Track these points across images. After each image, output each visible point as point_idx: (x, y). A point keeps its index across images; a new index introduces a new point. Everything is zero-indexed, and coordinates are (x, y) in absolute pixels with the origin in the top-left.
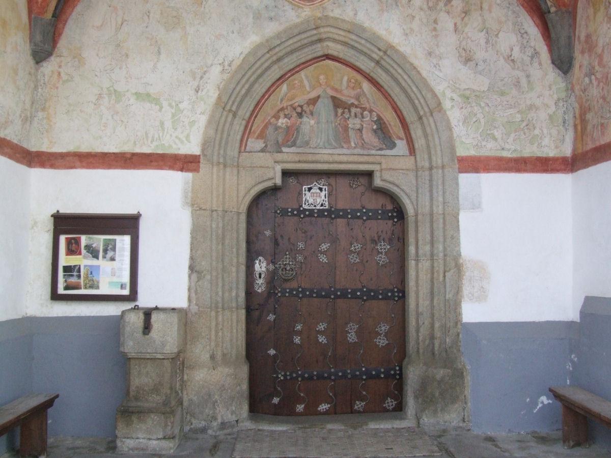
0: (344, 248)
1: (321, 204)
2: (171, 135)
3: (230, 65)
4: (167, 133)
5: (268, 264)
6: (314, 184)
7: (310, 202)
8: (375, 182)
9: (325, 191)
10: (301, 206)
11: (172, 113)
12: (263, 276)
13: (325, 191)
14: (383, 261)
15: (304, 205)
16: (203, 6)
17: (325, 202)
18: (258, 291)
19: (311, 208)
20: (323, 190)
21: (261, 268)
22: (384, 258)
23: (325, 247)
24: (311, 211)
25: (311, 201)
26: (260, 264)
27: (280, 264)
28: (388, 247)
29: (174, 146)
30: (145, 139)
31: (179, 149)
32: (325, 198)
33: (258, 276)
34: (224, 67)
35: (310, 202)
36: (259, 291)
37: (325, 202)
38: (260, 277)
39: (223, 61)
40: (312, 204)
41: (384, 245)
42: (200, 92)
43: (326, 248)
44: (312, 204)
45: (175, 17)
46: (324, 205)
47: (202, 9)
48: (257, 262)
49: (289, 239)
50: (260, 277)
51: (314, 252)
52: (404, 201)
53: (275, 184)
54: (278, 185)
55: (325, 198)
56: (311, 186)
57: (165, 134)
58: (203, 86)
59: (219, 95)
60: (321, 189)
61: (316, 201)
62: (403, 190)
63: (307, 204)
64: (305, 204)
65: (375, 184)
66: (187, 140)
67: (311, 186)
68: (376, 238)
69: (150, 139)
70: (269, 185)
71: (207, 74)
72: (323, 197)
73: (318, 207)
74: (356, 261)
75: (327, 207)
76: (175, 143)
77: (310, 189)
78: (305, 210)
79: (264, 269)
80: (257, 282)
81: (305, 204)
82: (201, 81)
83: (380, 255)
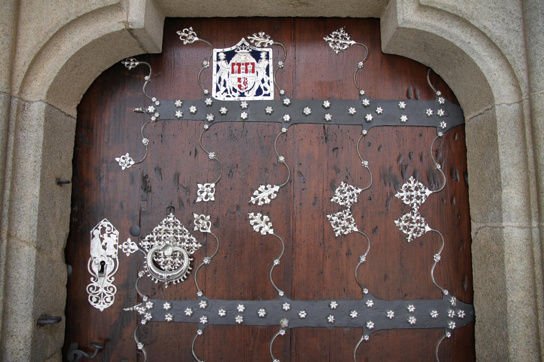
0: (315, 198)
1: (256, 87)
5: (122, 239)
6: (239, 44)
7: (229, 86)
8: (400, 17)
9: (267, 58)
10: (209, 95)
12: (109, 269)
13: (267, 58)
14: (415, 231)
15: (214, 94)
17: (266, 84)
18: (97, 306)
19: (232, 99)
20: (263, 55)
21: (104, 248)
22: (418, 221)
23: (265, 194)
24: (235, 106)
25: (232, 82)
26: (102, 239)
27: (150, 240)
28: (428, 192)
32: (268, 74)
33: (96, 269)
35: (229, 86)
36: (101, 307)
37: (266, 84)
38: (102, 271)
40: (235, 91)
41: (416, 189)
43: (269, 196)
44: (235, 91)
46: (264, 92)
48: (96, 232)
49: (177, 176)
50: (102, 271)
51: (238, 207)
52: (480, 65)
53: (127, 23)
54: (135, 27)
55: (268, 74)
56: (234, 48)
60: (256, 55)
61: (245, 83)
62: (482, 34)
63: (222, 89)
64: (218, 90)
65: (400, 22)
67: (234, 48)
68: (396, 171)
70: (114, 30)
72: (262, 74)
73: (251, 96)
74: (349, 230)
75: (271, 98)
77: (229, 56)
78: (217, 104)
79: (112, 251)
80: (95, 284)
81: (218, 90)
83: (409, 215)
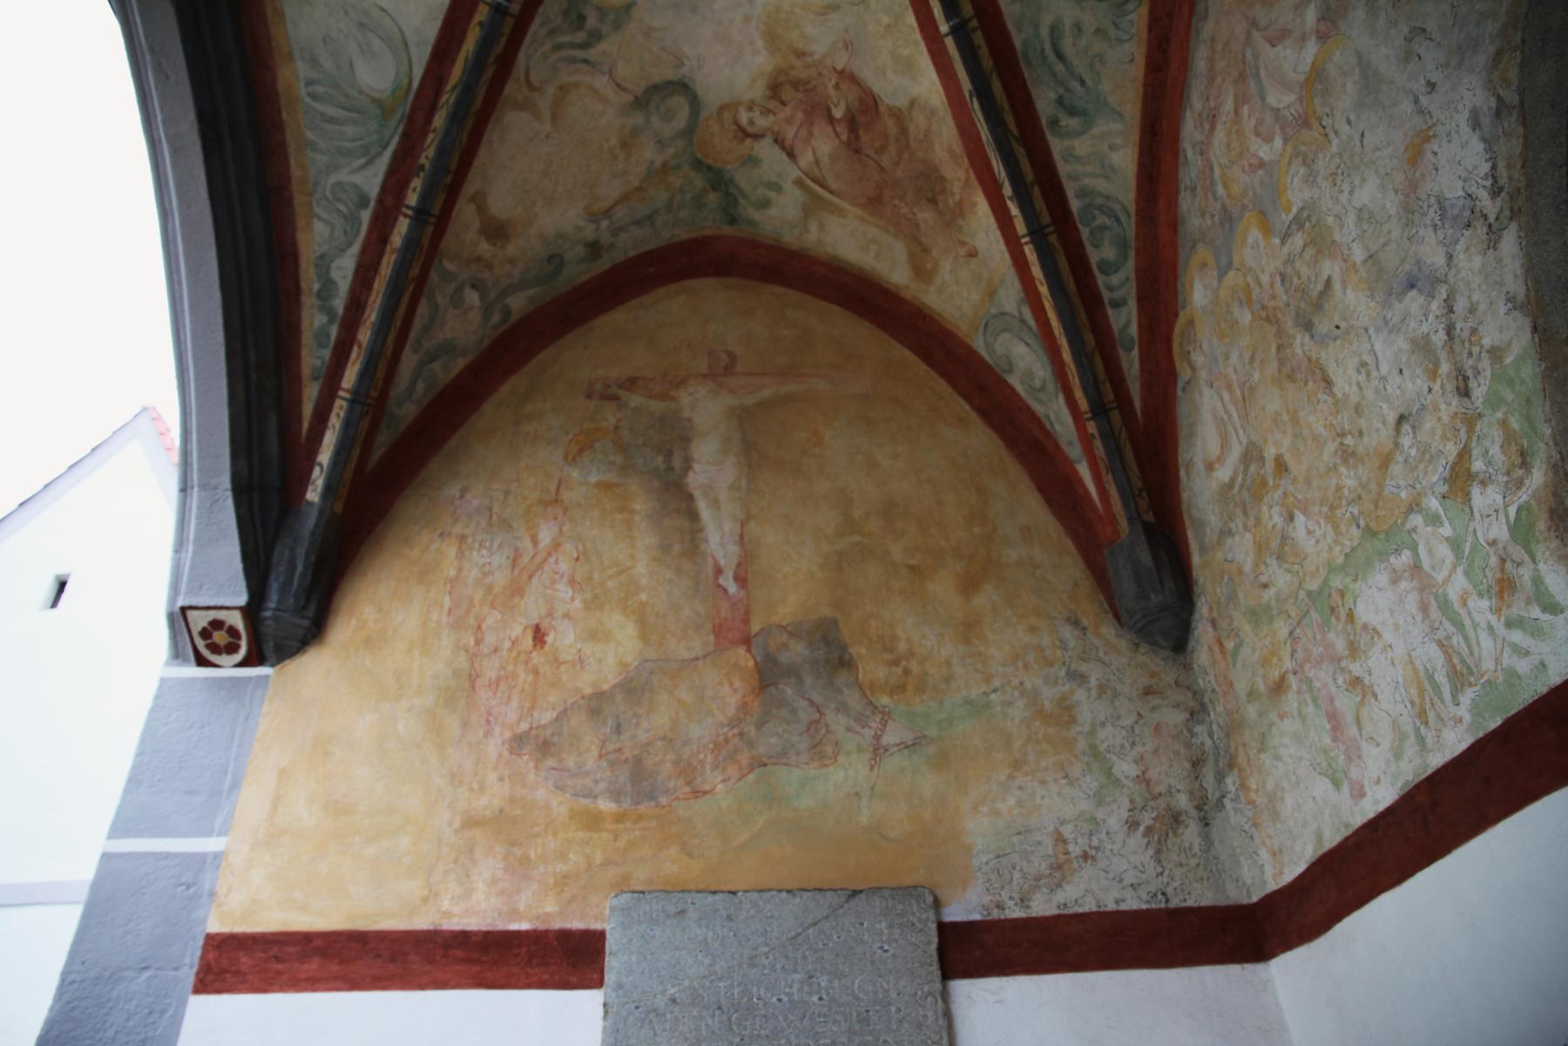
2: (1491, 628)
3: (1495, 192)
4: (1475, 626)
11: (1447, 539)
16: (1332, 135)
29: (1523, 666)
30: (1436, 699)
31: (1543, 665)
34: (1485, 217)
39: (1469, 203)
42: (1472, 384)
45: (1304, 247)
47: (1335, 141)
57: (1471, 634)
58: (1470, 354)
59: (1535, 329)
66: (1544, 609)
69: (1446, 691)
71: (1461, 304)
76: (1524, 653)
82: (1457, 348)
